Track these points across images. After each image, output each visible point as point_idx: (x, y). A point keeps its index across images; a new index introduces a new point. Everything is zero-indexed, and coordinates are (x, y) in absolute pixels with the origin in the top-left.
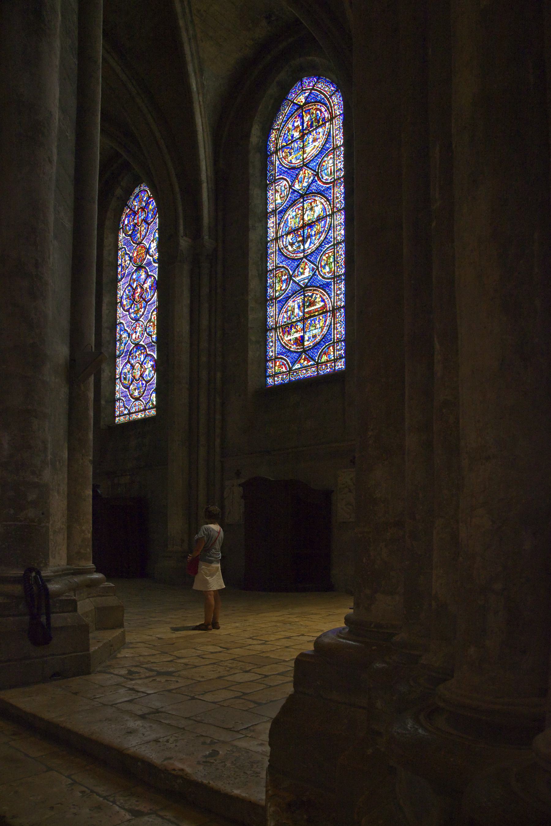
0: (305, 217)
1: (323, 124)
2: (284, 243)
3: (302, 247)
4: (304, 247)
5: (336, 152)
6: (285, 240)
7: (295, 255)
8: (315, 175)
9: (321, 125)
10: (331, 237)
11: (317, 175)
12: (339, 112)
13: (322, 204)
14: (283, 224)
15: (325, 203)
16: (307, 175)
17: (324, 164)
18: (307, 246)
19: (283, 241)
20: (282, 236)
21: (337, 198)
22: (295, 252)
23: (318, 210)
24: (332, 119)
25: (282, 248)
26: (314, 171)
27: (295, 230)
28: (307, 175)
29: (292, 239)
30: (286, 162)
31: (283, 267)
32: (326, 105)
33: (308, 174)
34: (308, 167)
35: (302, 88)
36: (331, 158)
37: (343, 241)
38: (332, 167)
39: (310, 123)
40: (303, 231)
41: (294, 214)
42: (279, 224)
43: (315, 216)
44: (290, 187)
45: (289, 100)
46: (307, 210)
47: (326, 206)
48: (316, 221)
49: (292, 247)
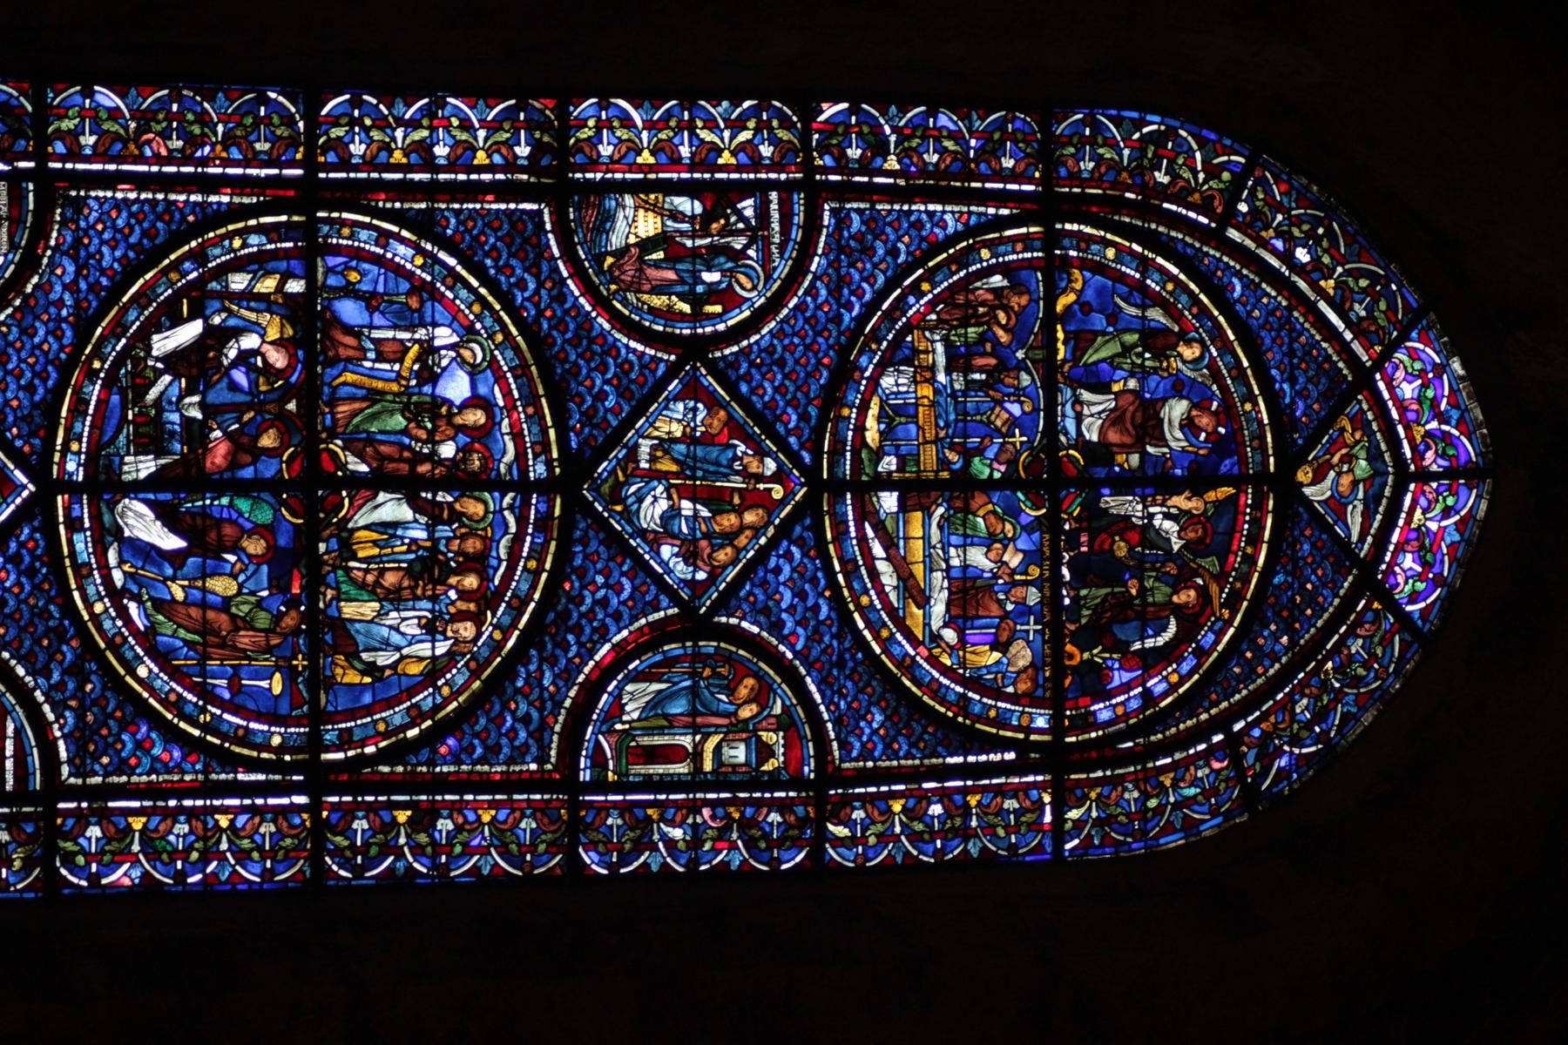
0: (392, 508)
1: (1060, 671)
2: (238, 282)
3: (144, 467)
4: (136, 488)
5: (783, 806)
6: (268, 285)
7: (95, 391)
8: (688, 609)
9: (1058, 654)
10: (122, 767)
11: (691, 624)
12: (1079, 824)
13: (436, 669)
14: (415, 265)
15: (424, 698)
16: (729, 521)
17: (747, 686)
18: (142, 522)
19: (257, 263)
20: (311, 250)
21: (424, 819)
22: (131, 377)
23: (402, 636)
24: (1055, 761)
25: (199, 257)
26: (725, 603)
27: (311, 391)
28: (729, 521)
29: (245, 357)
30: (915, 307)
31: (29, 264)
32: (1188, 704)
33: (729, 537)
34: (784, 531)
35: (1424, 476)
36: (766, 752)
37: (51, 880)
38: (681, 768)
39: (1121, 549)
40: (274, 486)
41: (456, 387)
42: (425, 226)
43: (358, 610)
44: (695, 349)
45: (1387, 354)
46: (434, 515)
47: (397, 715)
48: (313, 615)
49: (174, 362)
